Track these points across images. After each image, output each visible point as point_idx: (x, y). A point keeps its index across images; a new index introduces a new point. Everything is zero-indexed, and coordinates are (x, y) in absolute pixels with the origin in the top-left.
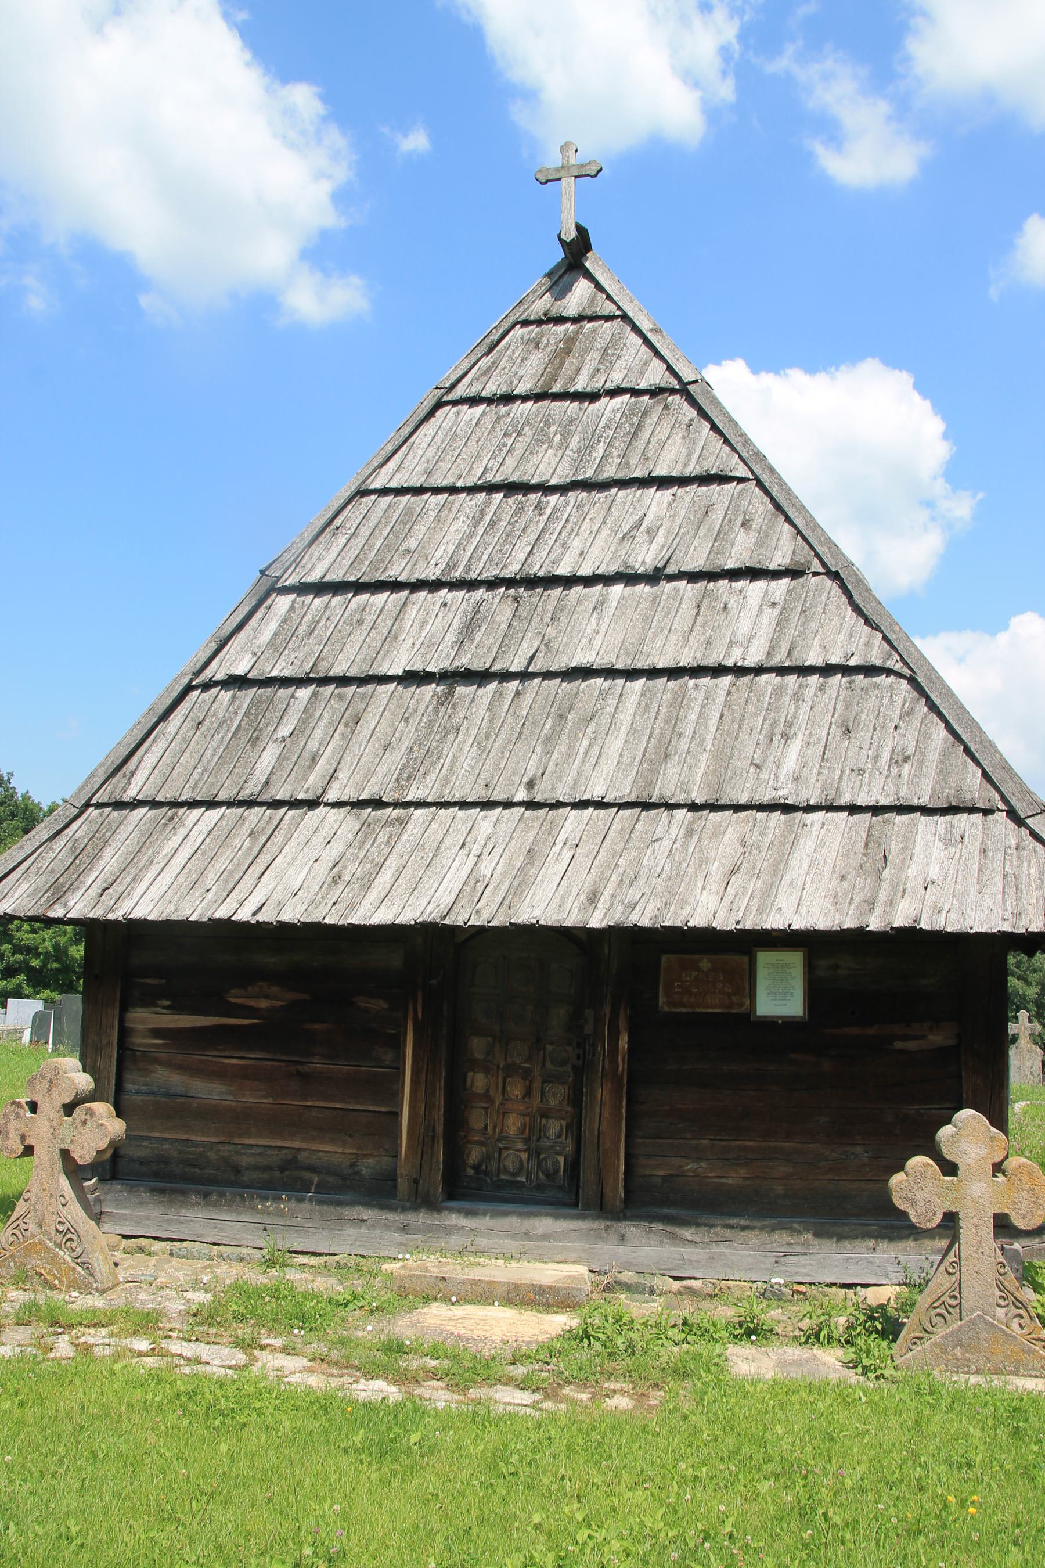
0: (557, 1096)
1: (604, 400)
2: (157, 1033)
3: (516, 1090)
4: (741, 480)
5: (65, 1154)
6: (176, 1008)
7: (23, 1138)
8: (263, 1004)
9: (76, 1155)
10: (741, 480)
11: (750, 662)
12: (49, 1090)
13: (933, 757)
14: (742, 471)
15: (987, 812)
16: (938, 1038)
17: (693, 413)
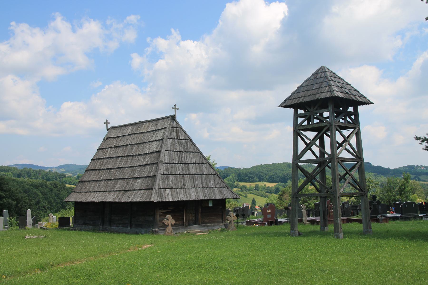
0: (194, 215)
1: (183, 140)
2: (162, 213)
3: (191, 215)
4: (198, 152)
5: (171, 224)
6: (163, 210)
7: (168, 223)
8: (171, 209)
9: (172, 224)
10: (198, 152)
11: (206, 174)
12: (170, 218)
13: (221, 183)
14: (198, 152)
15: (226, 188)
16: (221, 207)
17: (192, 143)
